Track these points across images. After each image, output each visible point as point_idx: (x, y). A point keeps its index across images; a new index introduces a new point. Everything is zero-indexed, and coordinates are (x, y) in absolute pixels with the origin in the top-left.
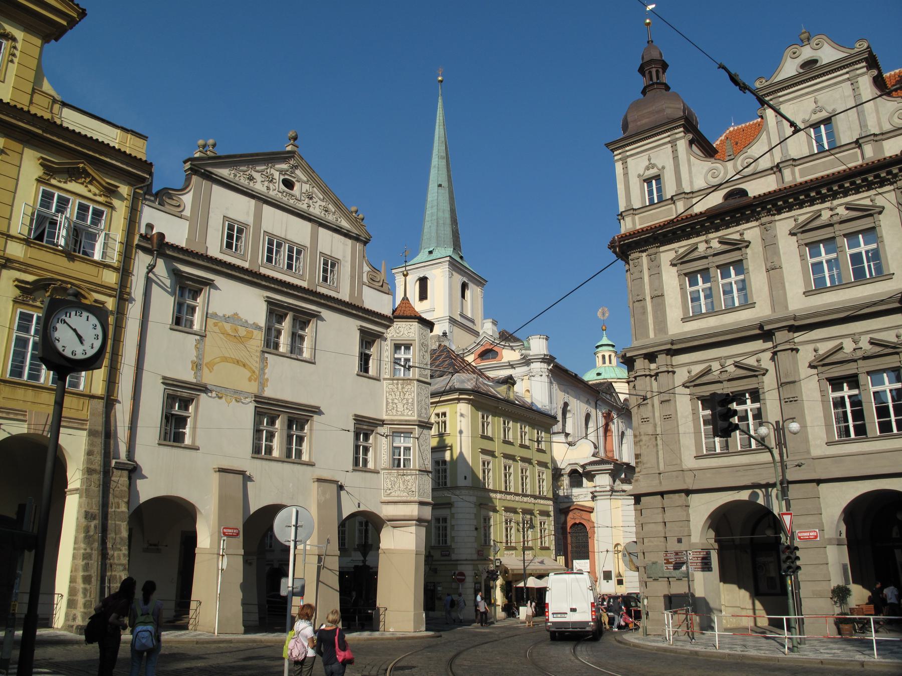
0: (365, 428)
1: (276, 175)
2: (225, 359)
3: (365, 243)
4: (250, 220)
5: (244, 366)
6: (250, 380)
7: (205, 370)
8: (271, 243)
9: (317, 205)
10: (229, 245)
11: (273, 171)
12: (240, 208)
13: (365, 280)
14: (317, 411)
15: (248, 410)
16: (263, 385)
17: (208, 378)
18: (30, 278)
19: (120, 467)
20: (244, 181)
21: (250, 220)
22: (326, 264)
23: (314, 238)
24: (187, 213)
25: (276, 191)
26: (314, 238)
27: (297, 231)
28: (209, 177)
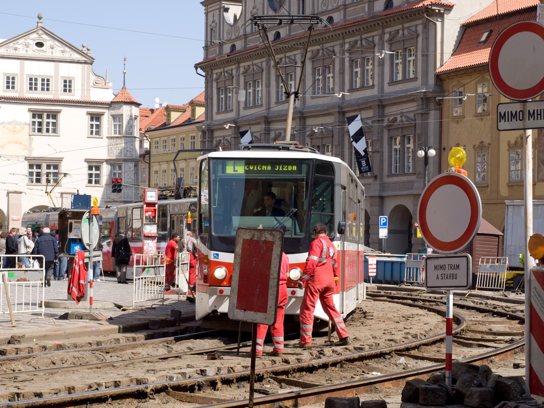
0: (94, 166)
3: (91, 64)
4: (18, 72)
5: (20, 143)
6: (24, 149)
9: (58, 51)
10: (8, 87)
11: (29, 41)
13: (92, 84)
14: (60, 160)
15: (26, 164)
16: (31, 151)
20: (11, 52)
22: (65, 81)
23: (57, 70)
25: (33, 51)
26: (57, 70)
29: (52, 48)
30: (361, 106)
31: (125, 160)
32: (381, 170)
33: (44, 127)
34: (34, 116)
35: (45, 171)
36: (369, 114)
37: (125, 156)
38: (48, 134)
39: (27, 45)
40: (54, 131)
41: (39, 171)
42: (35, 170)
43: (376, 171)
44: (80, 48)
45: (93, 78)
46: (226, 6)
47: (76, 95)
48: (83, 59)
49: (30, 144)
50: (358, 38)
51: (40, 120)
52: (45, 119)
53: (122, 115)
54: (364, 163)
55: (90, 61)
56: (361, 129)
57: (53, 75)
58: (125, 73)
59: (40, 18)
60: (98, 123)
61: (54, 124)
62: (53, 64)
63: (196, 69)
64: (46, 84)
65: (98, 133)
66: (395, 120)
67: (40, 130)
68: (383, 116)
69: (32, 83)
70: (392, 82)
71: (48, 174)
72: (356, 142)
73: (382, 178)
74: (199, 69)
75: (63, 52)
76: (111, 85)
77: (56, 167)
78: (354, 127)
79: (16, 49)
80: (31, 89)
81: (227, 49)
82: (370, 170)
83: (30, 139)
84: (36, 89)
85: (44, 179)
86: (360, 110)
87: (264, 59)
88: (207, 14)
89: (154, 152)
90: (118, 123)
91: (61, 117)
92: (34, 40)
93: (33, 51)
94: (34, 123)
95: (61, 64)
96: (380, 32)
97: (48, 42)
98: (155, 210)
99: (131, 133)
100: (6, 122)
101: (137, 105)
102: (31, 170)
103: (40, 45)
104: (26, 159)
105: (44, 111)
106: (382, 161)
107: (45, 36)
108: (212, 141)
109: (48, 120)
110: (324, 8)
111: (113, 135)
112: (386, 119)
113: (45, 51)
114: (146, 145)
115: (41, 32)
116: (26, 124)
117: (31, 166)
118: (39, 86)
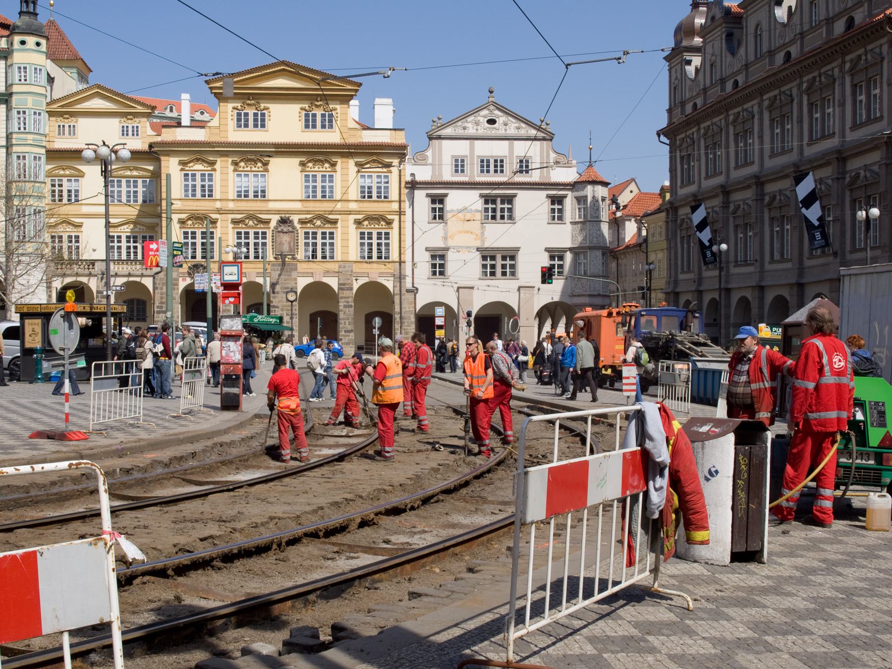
0: (556, 254)
1: (481, 119)
2: (461, 232)
3: (551, 140)
4: (467, 153)
7: (449, 239)
8: (482, 161)
10: (457, 171)
11: (479, 118)
12: (460, 148)
14: (517, 250)
15: (478, 256)
16: (483, 241)
17: (450, 243)
18: (360, 217)
19: (408, 291)
20: (460, 132)
21: (467, 153)
23: (511, 150)
24: (430, 161)
25: (484, 129)
26: (511, 150)
27: (498, 149)
28: (439, 138)
29: (506, 125)
30: (816, 164)
31: (590, 248)
32: (843, 243)
33: (499, 214)
34: (486, 202)
35: (499, 262)
36: (826, 172)
37: (591, 242)
38: (502, 221)
39: (477, 123)
40: (511, 217)
41: (493, 262)
42: (489, 262)
43: (836, 246)
44: (539, 123)
45: (553, 156)
46: (688, 58)
47: (535, 176)
48: (540, 135)
49: (483, 233)
50: (816, 74)
51: (494, 206)
52: (498, 204)
53: (586, 196)
54: (818, 235)
55: (549, 137)
56: (814, 191)
57: (507, 154)
58: (591, 149)
59: (491, 92)
60: (560, 207)
61: (510, 210)
62: (507, 142)
63: (659, 136)
64: (499, 165)
65: (560, 218)
66: (858, 175)
67: (494, 217)
68: (845, 173)
69: (484, 165)
70: (855, 127)
71: (504, 266)
72: (807, 209)
73: (844, 255)
74: (662, 136)
75: (518, 128)
76: (574, 162)
77: (513, 258)
78: (804, 188)
79: (465, 128)
80: (482, 171)
81: (689, 108)
82: (827, 244)
83: (483, 228)
84: (488, 171)
85: (499, 270)
86: (814, 169)
87: (722, 116)
88: (670, 70)
89: (650, 240)
90: (582, 206)
91: (517, 202)
92: (485, 117)
93: (484, 129)
94: (486, 210)
95: (515, 142)
96: (839, 61)
97: (501, 119)
98: (239, 294)
99: (598, 217)
100: (455, 209)
101: (605, 184)
102: (485, 263)
103: (492, 122)
104: (478, 249)
105: (497, 196)
106: (843, 233)
107: (497, 112)
108: (676, 221)
109: (503, 206)
110: (781, 42)
111: (577, 220)
112: (848, 176)
113: (499, 129)
114: (644, 233)
115: (492, 107)
116: (477, 211)
117: (484, 258)
118: (492, 168)
